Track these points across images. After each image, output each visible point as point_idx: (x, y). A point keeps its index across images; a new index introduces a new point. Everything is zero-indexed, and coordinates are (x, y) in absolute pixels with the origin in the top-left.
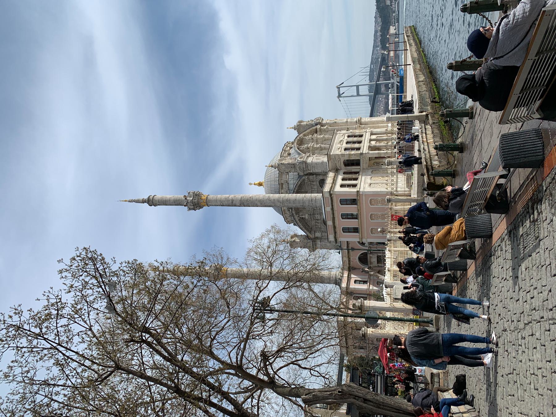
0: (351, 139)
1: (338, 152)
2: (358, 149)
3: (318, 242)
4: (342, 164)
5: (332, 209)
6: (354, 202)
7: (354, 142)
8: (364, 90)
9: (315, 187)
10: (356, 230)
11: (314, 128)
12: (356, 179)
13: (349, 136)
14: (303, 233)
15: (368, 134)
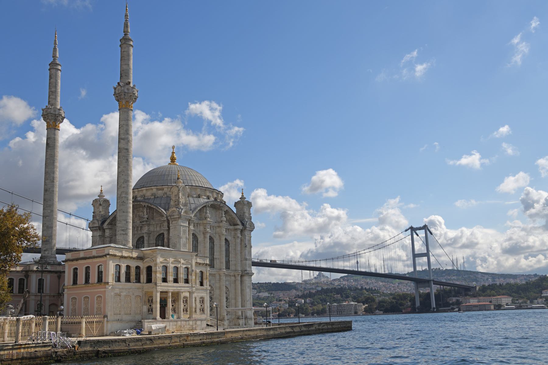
1: (160, 260)
3: (98, 233)
5: (94, 257)
6: (100, 280)
8: (422, 264)
9: (158, 229)
10: (75, 282)
11: (239, 222)
12: (128, 280)
14: (110, 214)
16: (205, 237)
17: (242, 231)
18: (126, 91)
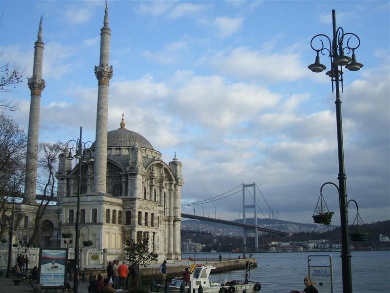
0: (150, 216)
2: (140, 223)
4: (128, 210)
7: (146, 219)
8: (250, 215)
9: (116, 181)
11: (173, 178)
12: (114, 222)
13: (152, 214)
15: (154, 230)
16: (151, 189)
17: (175, 185)
18: (106, 70)
